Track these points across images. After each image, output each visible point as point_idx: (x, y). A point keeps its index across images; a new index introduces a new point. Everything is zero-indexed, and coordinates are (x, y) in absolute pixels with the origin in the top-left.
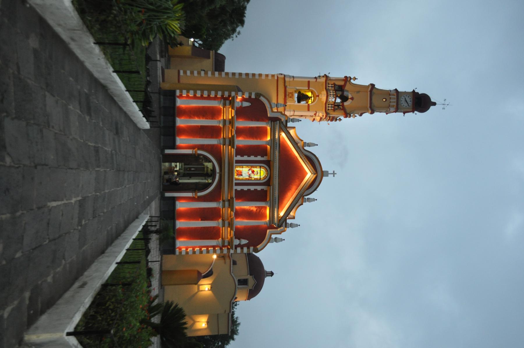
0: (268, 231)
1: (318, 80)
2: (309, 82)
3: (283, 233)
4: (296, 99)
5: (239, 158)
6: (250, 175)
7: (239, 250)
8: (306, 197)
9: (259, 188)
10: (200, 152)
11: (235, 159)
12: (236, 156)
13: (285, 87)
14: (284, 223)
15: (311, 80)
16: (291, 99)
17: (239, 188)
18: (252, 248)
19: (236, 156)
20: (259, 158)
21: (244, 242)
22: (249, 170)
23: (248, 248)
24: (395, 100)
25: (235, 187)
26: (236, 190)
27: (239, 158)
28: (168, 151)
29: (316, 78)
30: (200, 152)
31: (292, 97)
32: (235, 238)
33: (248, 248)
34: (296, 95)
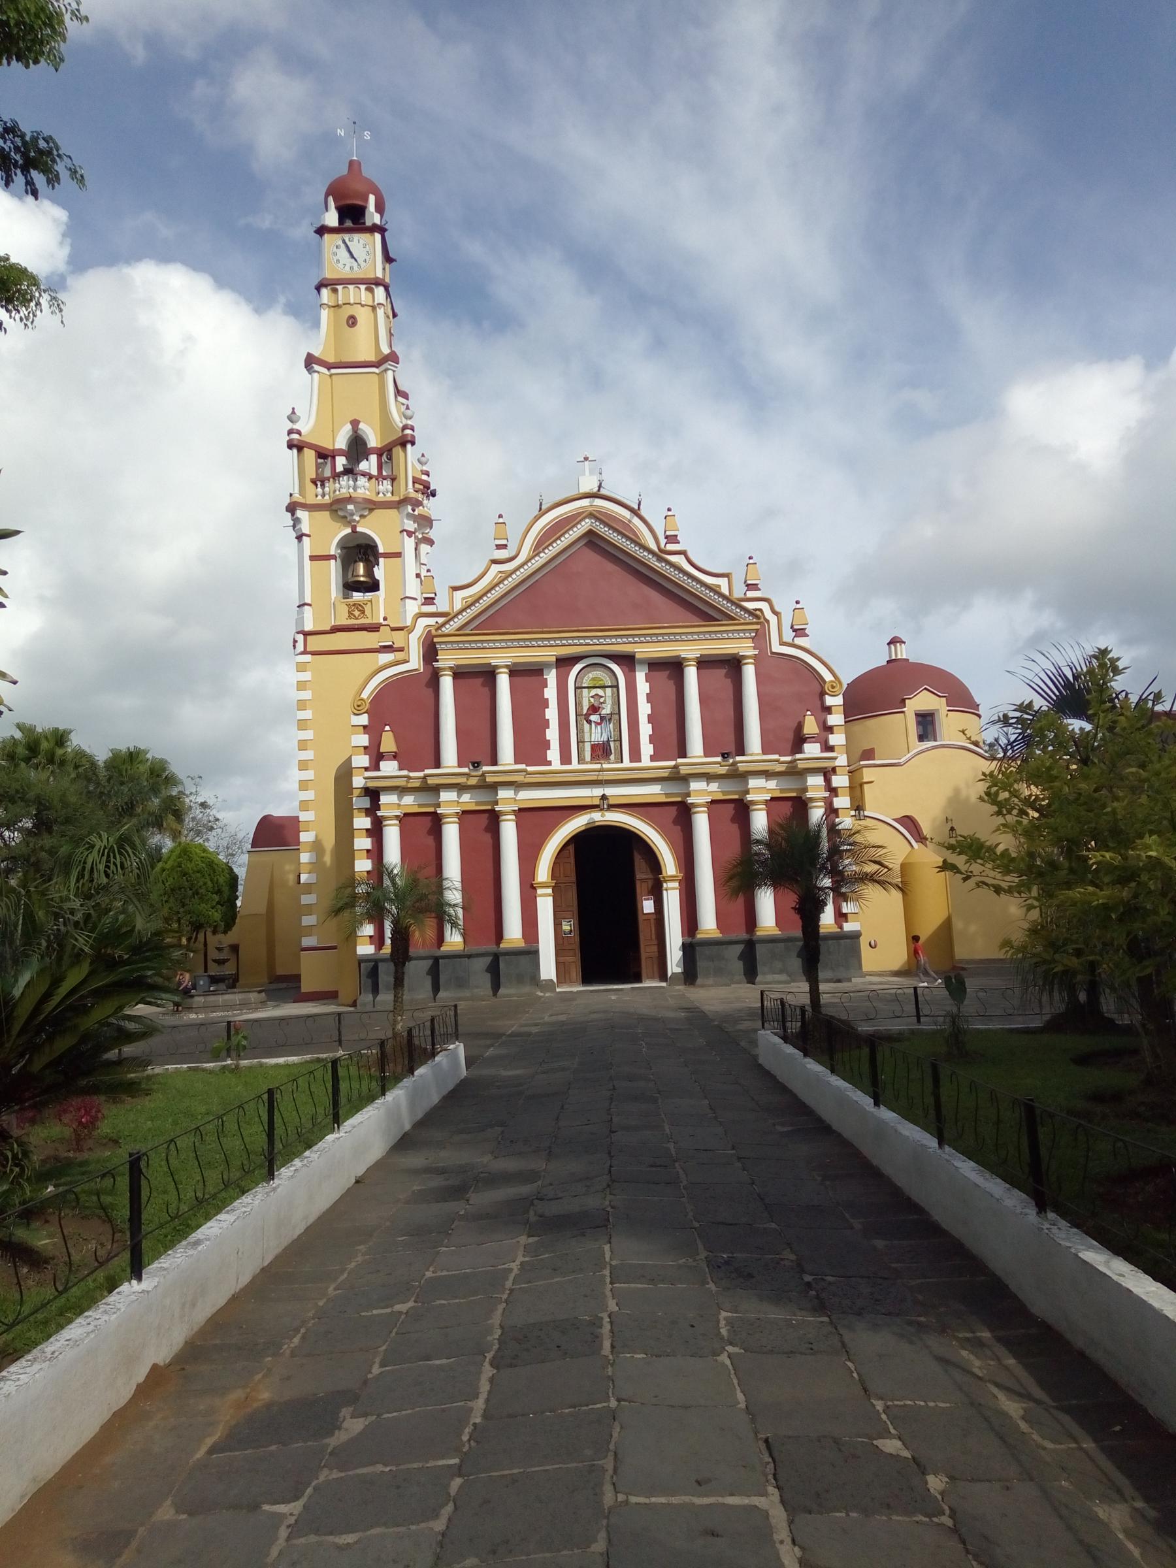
0: (777, 648)
1: (306, 530)
2: (313, 558)
3: (777, 609)
4: (369, 595)
5: (553, 754)
6: (602, 718)
7: (837, 739)
8: (663, 541)
9: (643, 687)
10: (543, 872)
11: (556, 765)
12: (549, 763)
13: (335, 630)
14: (746, 604)
15: (307, 553)
16: (367, 609)
17: (647, 749)
18: (829, 701)
19: (549, 763)
20: (551, 693)
21: (811, 726)
22: (589, 722)
23: (828, 710)
24: (351, 287)
25: (646, 761)
26: (653, 758)
27: (553, 754)
28: (548, 969)
29: (299, 538)
30: (543, 872)
31: (359, 607)
32: (801, 751)
33: (828, 710)
34: (357, 596)
